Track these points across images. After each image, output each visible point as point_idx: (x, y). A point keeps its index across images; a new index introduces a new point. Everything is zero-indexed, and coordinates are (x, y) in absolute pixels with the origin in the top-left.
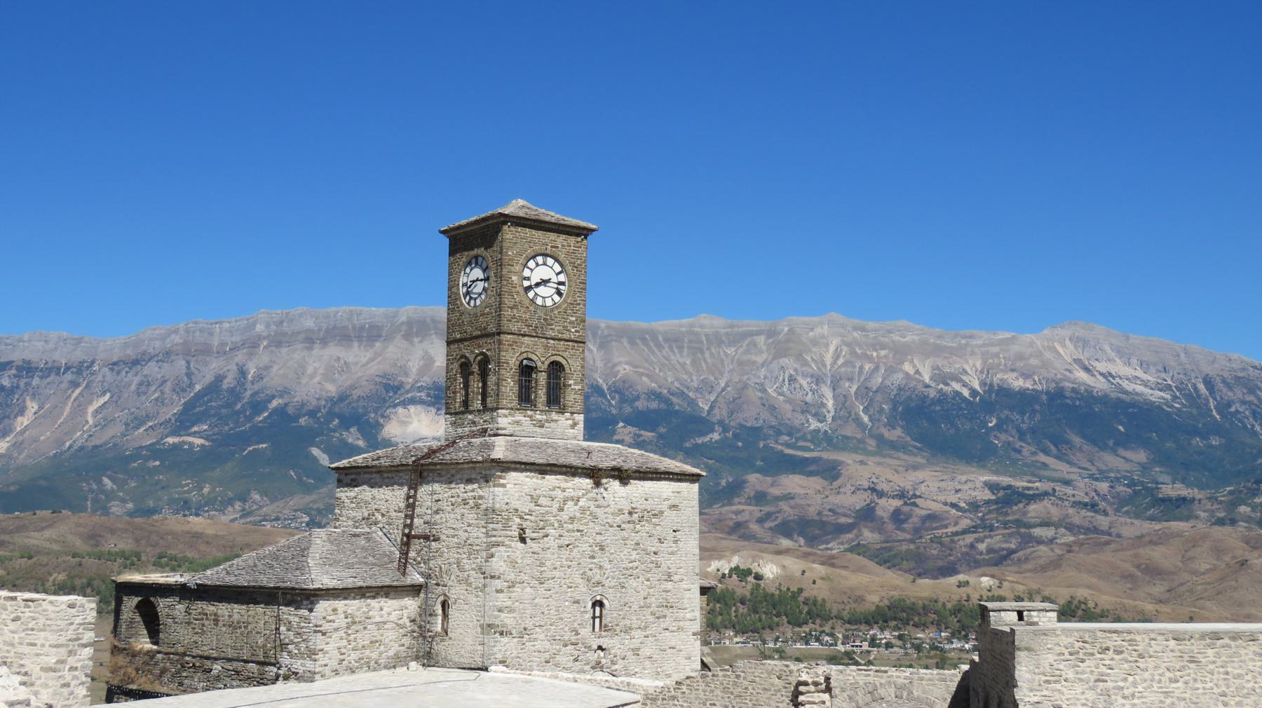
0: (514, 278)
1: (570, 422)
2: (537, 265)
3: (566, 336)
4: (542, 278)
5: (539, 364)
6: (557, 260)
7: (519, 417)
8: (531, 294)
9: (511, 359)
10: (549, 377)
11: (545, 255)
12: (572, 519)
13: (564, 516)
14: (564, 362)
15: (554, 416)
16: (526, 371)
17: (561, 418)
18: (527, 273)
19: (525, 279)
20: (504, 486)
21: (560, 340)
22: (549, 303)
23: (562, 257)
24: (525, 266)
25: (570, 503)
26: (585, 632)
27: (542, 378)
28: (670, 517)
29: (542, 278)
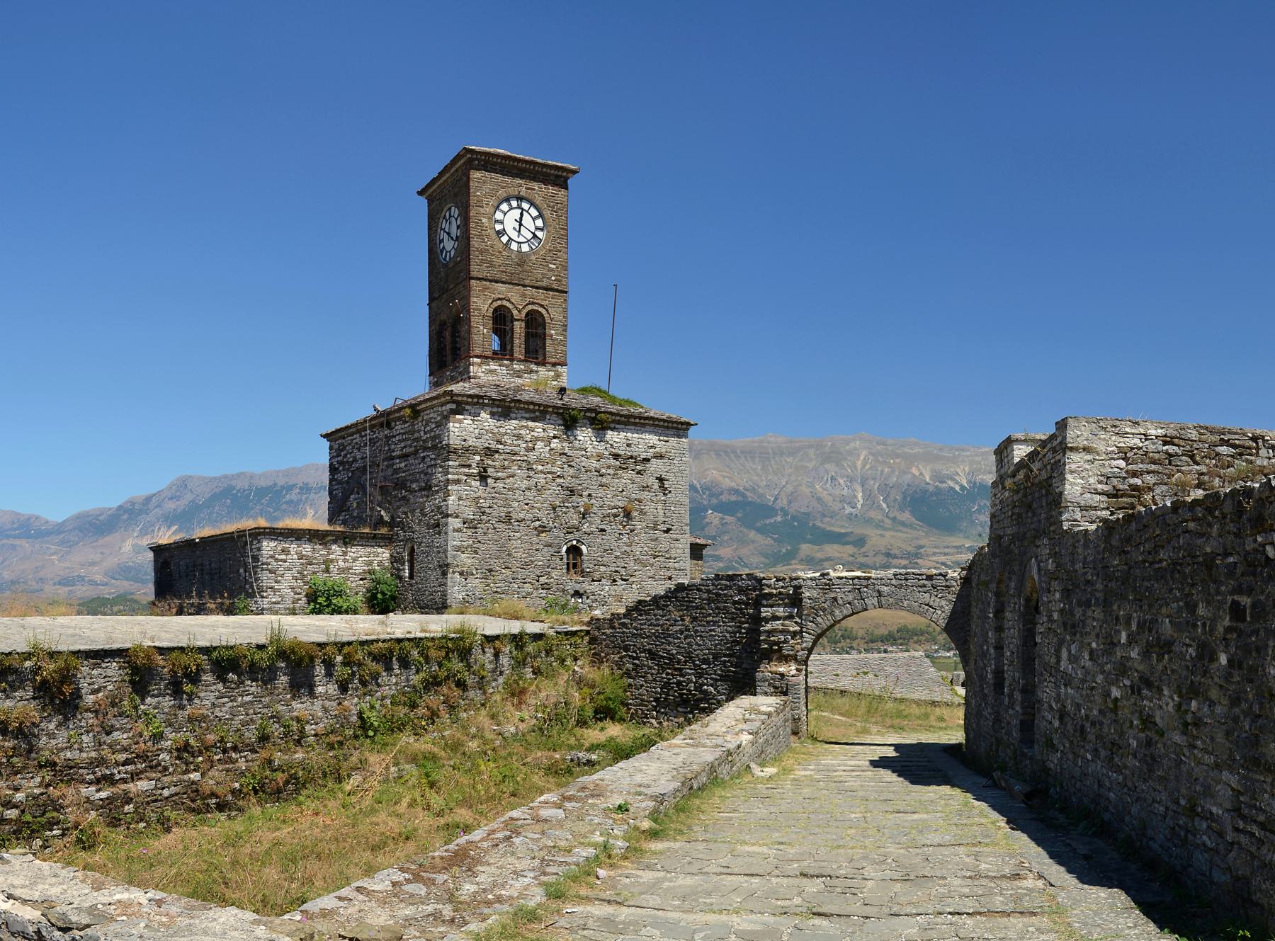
0: (484, 220)
1: (552, 373)
2: (511, 208)
3: (543, 284)
4: (515, 224)
5: (515, 312)
6: (532, 204)
7: (493, 366)
8: (504, 239)
9: (481, 304)
10: (527, 327)
11: (519, 198)
12: (540, 461)
13: (532, 457)
14: (543, 311)
15: (534, 367)
16: (501, 319)
17: (542, 370)
18: (499, 216)
19: (497, 221)
20: (460, 422)
21: (537, 288)
22: (525, 248)
23: (538, 201)
24: (497, 208)
25: (540, 444)
26: (557, 574)
27: (519, 328)
28: (656, 467)
29: (515, 224)
